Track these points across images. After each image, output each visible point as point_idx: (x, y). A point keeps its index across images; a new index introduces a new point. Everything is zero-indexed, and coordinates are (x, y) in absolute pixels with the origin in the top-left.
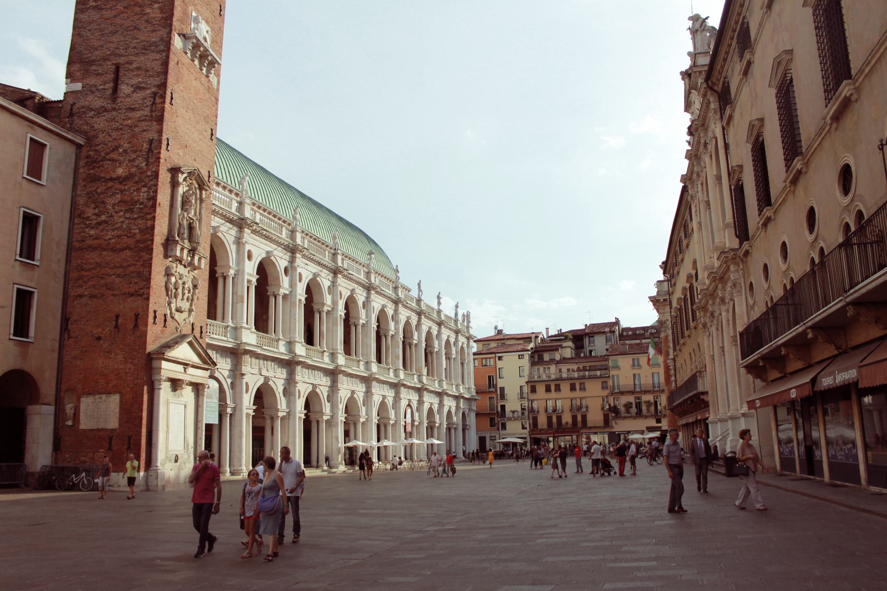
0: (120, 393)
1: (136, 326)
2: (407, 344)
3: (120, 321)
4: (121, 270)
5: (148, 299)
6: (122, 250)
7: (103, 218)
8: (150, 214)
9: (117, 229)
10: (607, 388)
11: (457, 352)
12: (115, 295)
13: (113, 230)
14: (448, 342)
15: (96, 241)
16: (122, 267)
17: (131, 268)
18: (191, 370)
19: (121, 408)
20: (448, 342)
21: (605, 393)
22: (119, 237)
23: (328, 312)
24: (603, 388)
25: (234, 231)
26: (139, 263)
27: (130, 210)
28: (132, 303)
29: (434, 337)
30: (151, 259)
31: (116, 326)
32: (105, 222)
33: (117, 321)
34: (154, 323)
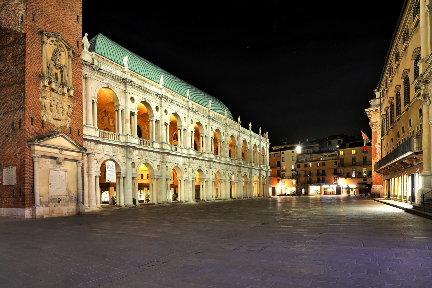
0: (16, 165)
1: (20, 127)
2: (216, 141)
3: (14, 125)
4: (13, 96)
5: (24, 110)
6: (14, 84)
7: (6, 68)
8: (23, 60)
9: (11, 73)
10: (337, 164)
11: (260, 150)
12: (12, 111)
13: (10, 74)
14: (255, 145)
15: (5, 82)
16: (14, 94)
17: (18, 94)
18: (65, 152)
19: (17, 173)
20: (255, 145)
21: (335, 167)
22: (12, 77)
23: (184, 130)
24: (335, 165)
25: (122, 87)
26: (20, 90)
27: (15, 61)
28: (19, 114)
29: (248, 143)
30: (25, 87)
31: (13, 129)
32: (7, 70)
33: (13, 126)
34: (32, 124)
